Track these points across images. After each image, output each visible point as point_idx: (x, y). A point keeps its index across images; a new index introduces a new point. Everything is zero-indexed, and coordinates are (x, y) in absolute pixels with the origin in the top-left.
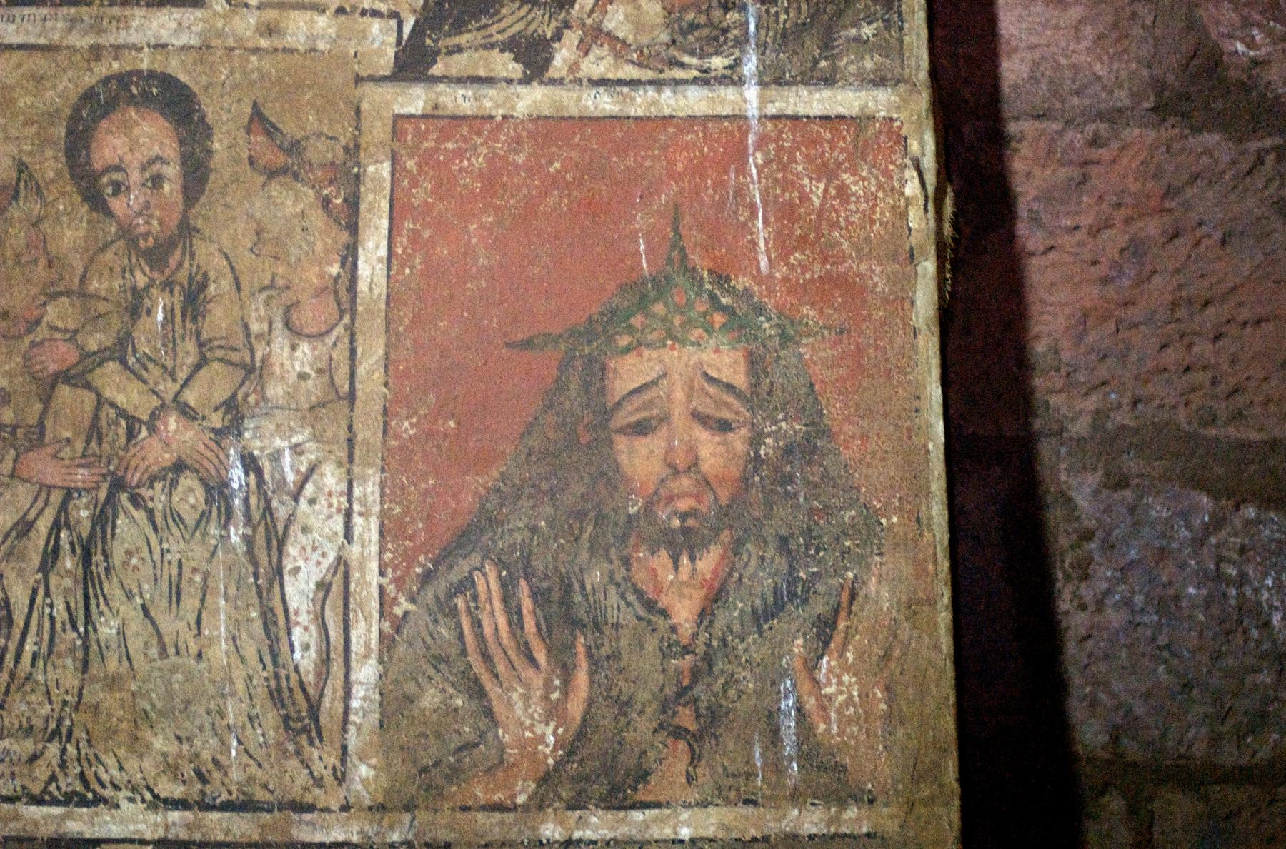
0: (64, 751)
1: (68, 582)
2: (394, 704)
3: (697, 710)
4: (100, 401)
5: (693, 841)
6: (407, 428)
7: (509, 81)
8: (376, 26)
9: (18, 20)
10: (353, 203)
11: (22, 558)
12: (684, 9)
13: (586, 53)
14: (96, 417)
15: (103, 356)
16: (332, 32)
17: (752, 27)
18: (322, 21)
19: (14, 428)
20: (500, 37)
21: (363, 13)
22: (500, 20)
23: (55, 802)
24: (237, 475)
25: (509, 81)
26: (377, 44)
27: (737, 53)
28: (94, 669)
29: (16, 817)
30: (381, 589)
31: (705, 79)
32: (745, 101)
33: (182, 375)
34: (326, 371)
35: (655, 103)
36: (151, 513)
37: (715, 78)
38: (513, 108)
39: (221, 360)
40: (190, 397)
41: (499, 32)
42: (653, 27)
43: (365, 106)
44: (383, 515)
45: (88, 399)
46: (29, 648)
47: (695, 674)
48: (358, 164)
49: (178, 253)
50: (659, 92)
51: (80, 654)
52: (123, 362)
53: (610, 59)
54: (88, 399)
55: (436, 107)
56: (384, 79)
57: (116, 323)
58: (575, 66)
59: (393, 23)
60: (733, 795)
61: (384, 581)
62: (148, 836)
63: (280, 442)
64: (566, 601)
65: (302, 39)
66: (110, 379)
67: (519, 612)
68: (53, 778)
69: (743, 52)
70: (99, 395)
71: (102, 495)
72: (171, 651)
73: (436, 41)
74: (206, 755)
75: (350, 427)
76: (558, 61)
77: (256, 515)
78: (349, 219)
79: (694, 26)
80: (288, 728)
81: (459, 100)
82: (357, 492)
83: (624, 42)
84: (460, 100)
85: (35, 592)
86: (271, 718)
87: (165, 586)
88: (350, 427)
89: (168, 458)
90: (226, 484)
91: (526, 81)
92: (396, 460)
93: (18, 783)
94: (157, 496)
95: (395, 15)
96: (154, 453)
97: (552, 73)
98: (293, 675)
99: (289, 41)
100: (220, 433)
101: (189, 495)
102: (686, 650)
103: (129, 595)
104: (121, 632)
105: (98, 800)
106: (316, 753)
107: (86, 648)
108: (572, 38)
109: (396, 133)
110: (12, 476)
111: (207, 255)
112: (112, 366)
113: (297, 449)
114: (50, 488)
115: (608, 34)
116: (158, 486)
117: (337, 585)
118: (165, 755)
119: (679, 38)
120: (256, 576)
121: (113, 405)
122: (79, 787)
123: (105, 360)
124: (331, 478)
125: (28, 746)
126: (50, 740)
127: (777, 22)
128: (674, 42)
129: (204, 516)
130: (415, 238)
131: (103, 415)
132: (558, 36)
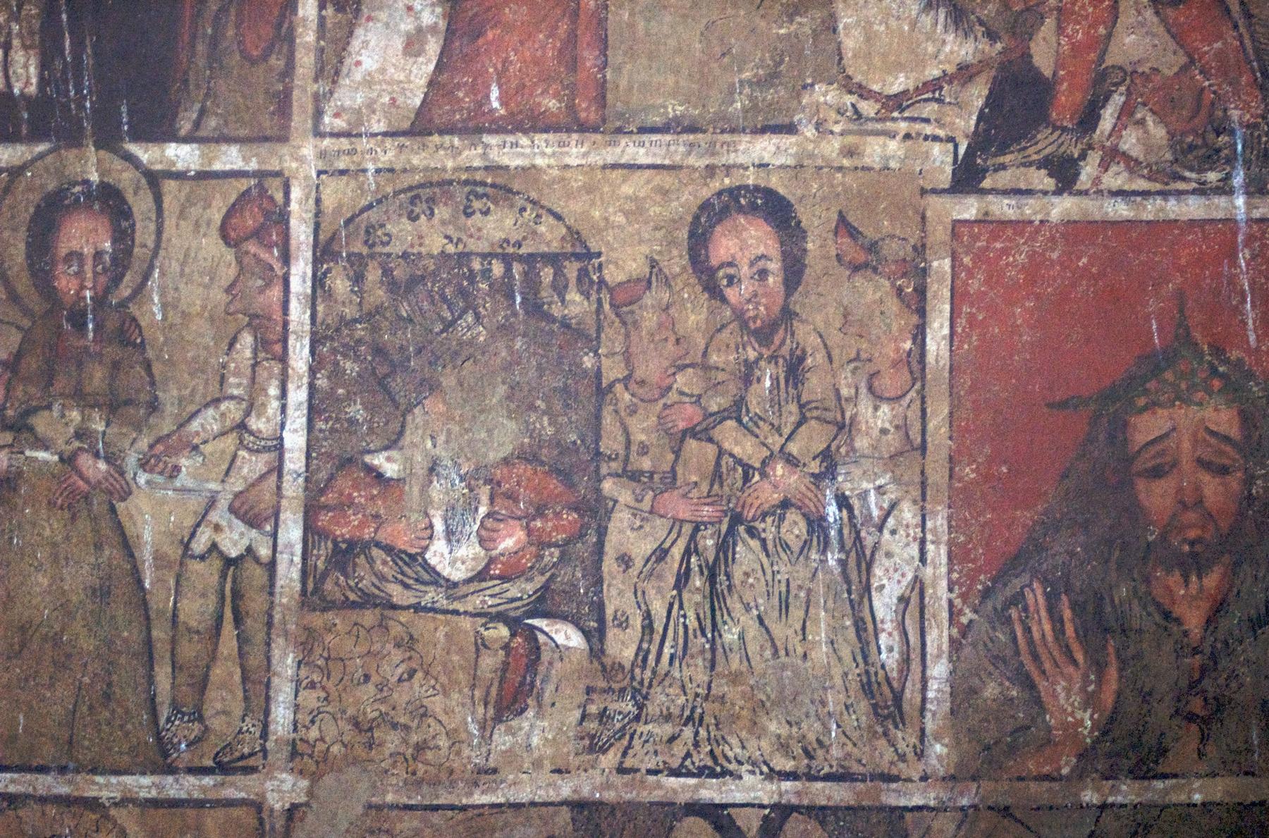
0: (697, 733)
1: (698, 598)
2: (963, 693)
3: (1205, 699)
4: (721, 453)
5: (1204, 804)
6: (969, 472)
8: (936, 149)
10: (921, 291)
11: (660, 577)
12: (1183, 134)
13: (1106, 170)
14: (718, 464)
15: (722, 415)
16: (901, 153)
17: (1240, 147)
18: (893, 145)
19: (652, 474)
20: (1035, 157)
21: (926, 138)
22: (1036, 143)
23: (689, 774)
24: (832, 511)
25: (1045, 193)
26: (938, 164)
27: (1228, 169)
28: (719, 669)
29: (659, 786)
30: (950, 603)
31: (1203, 190)
32: (1235, 208)
33: (786, 431)
34: (903, 428)
35: (1162, 210)
36: (764, 542)
37: (1211, 189)
38: (1048, 214)
39: (817, 418)
40: (793, 448)
41: (1038, 153)
42: (1160, 148)
43: (929, 214)
44: (950, 543)
45: (711, 450)
46: (667, 651)
47: (1203, 670)
48: (925, 260)
49: (781, 332)
50: (1166, 200)
51: (708, 656)
52: (739, 421)
53: (1126, 174)
54: (711, 450)
55: (986, 214)
56: (943, 191)
57: (733, 388)
59: (950, 146)
60: (1235, 768)
61: (953, 596)
62: (766, 802)
63: (867, 485)
64: (1099, 611)
65: (877, 159)
66: (728, 434)
67: (1062, 621)
68: (688, 755)
69: (1233, 168)
70: (720, 448)
71: (724, 527)
72: (782, 653)
73: (985, 161)
74: (812, 737)
75: (923, 473)
76: (1083, 177)
77: (849, 544)
78: (919, 305)
79: (1192, 147)
80: (876, 714)
81: (1005, 208)
82: (929, 524)
83: (1136, 160)
84: (1006, 208)
85: (671, 605)
86: (863, 706)
87: (776, 601)
88: (923, 473)
89: (776, 497)
90: (823, 518)
92: (961, 498)
93: (660, 758)
94: (768, 528)
95: (951, 139)
96: (765, 494)
97: (1078, 186)
98: (881, 672)
99: (867, 161)
100: (817, 477)
101: (794, 528)
102: (1196, 651)
103: (747, 608)
104: (742, 637)
105: (725, 773)
106: (900, 734)
107: (713, 650)
109: (955, 234)
110: (651, 512)
111: (806, 335)
112: (731, 423)
113: (880, 490)
114: (682, 521)
115: (1124, 153)
116: (769, 520)
117: (914, 599)
118: (779, 737)
119: (1180, 157)
120: (849, 592)
121: (732, 455)
122: (710, 763)
123: (724, 419)
124: (908, 513)
125: (668, 729)
126: (685, 725)
127: (1259, 143)
128: (1177, 160)
129: (806, 545)
130: (971, 320)
131: (723, 463)
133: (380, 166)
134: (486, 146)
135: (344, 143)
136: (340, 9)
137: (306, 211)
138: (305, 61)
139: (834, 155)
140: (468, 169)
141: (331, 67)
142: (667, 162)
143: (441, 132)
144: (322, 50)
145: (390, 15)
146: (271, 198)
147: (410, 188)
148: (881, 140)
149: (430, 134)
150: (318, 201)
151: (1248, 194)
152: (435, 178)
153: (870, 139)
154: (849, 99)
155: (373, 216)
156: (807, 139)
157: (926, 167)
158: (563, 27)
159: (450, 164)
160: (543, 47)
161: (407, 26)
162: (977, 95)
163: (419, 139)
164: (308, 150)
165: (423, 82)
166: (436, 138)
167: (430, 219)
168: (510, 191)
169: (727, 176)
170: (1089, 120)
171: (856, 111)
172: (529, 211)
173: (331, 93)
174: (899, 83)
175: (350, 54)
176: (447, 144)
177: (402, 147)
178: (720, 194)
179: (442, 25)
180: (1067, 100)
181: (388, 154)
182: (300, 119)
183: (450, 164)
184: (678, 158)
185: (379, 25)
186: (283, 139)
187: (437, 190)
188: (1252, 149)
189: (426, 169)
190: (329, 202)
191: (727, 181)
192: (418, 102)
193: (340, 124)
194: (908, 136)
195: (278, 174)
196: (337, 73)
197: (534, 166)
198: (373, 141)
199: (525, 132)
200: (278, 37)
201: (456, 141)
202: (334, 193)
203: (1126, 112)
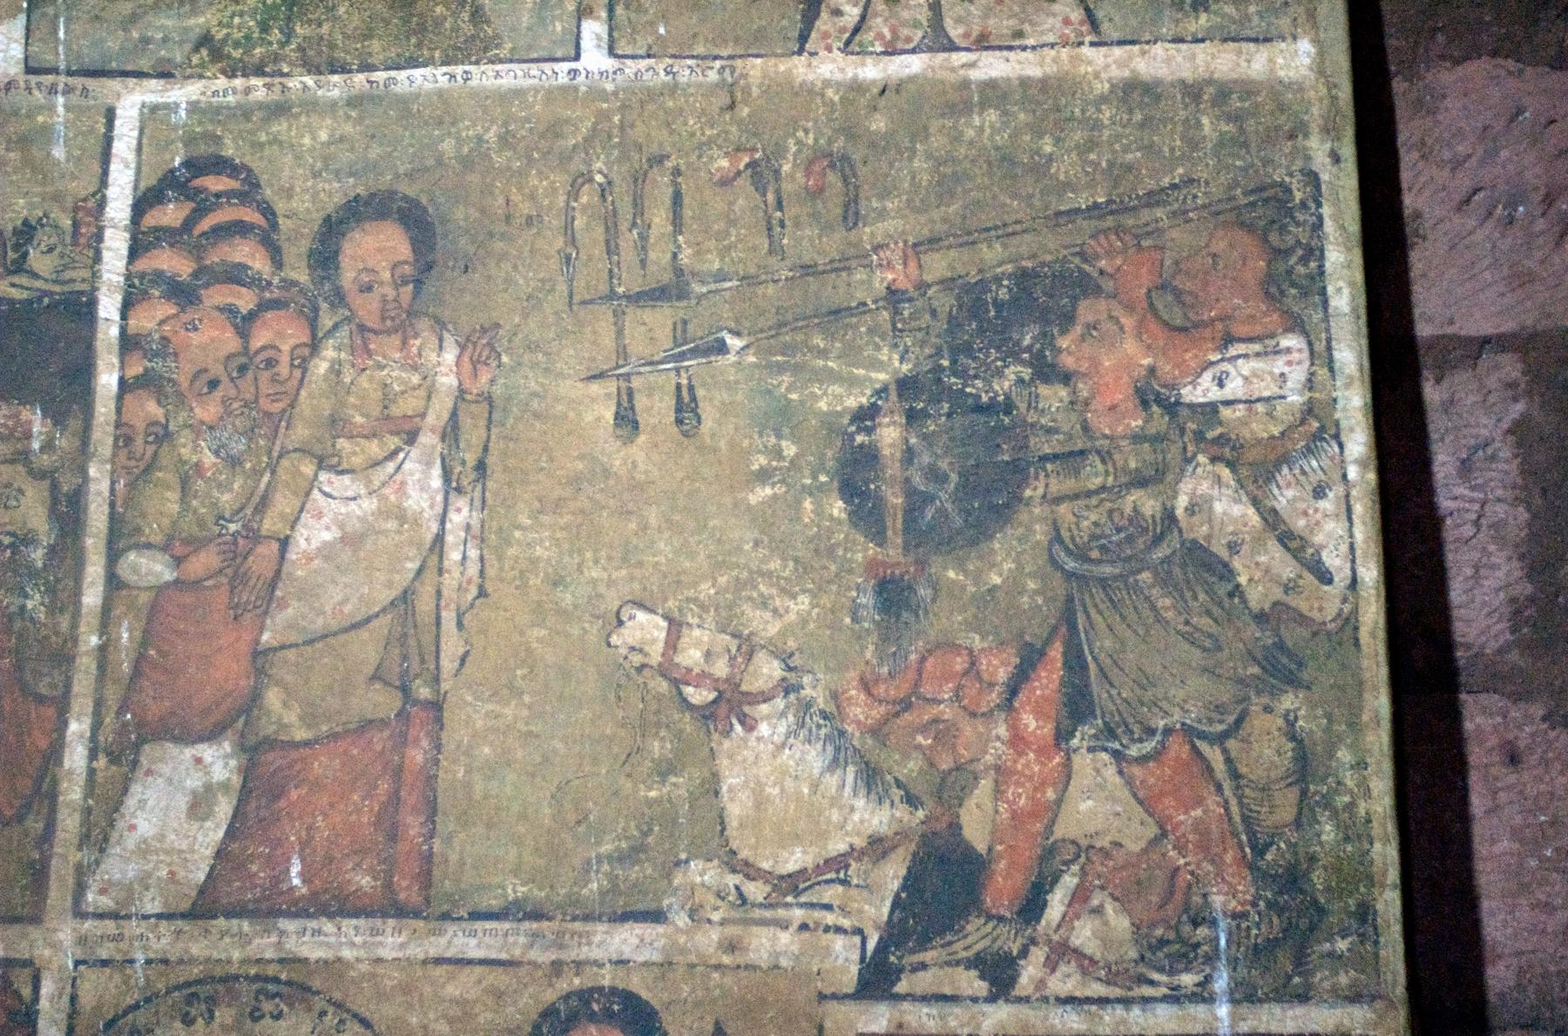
7: (975, 1000)
8: (839, 943)
9: (480, 934)
12: (1153, 925)
13: (1053, 970)
16: (795, 948)
18: (785, 938)
20: (965, 954)
21: (827, 929)
22: (965, 937)
25: (975, 1000)
26: (840, 961)
27: (1208, 970)
31: (1175, 997)
32: (1216, 1019)
35: (1124, 1022)
37: (1185, 996)
38: (979, 1026)
41: (965, 949)
42: (1121, 945)
43: (828, 1024)
50: (1127, 1010)
53: (1079, 977)
55: (900, 1026)
56: (846, 996)
58: (1041, 984)
59: (857, 940)
65: (765, 956)
69: (1214, 969)
73: (900, 958)
76: (1024, 979)
79: (1163, 942)
83: (1091, 959)
84: (925, 1019)
91: (992, 999)
95: (859, 931)
97: (1018, 991)
99: (752, 957)
108: (1038, 954)
115: (1075, 951)
119: (1148, 955)
128: (1142, 958)
132: (1024, 953)
133: (152, 956)
134: (282, 933)
135: (110, 926)
136: (114, 759)
137: (58, 1010)
138: (69, 824)
139: (712, 950)
140: (259, 961)
141: (99, 830)
142: (504, 956)
143: (229, 915)
144: (88, 811)
145: (175, 769)
146: (17, 995)
147: (188, 984)
148: (769, 931)
149: (214, 917)
150: (73, 999)
151: (1234, 1002)
152: (218, 972)
153: (755, 929)
154: (732, 880)
155: (141, 1018)
156: (678, 930)
157: (827, 966)
158: (384, 786)
159: (236, 955)
160: (358, 811)
161: (194, 782)
162: (892, 874)
163: (200, 922)
164: (66, 934)
165: (209, 852)
166: (221, 922)
167: (208, 1024)
168: (309, 989)
169: (577, 974)
170: (1032, 907)
171: (741, 895)
172: (330, 1017)
173: (98, 863)
174: (795, 860)
175: (123, 816)
176: (235, 930)
177: (179, 932)
178: (567, 997)
179: (236, 781)
180: (1003, 887)
181: (163, 941)
182: (58, 895)
183: (236, 955)
184: (517, 952)
185: (160, 780)
186: (36, 919)
187: (220, 988)
188: (1239, 945)
189: (208, 960)
190: (87, 1000)
191: (577, 981)
192: (201, 876)
193: (106, 902)
194: (804, 927)
195: (28, 963)
196: (106, 840)
197: (339, 959)
198: (144, 923)
199: (331, 916)
200: (37, 789)
201: (246, 926)
202: (93, 987)
203: (1079, 897)
